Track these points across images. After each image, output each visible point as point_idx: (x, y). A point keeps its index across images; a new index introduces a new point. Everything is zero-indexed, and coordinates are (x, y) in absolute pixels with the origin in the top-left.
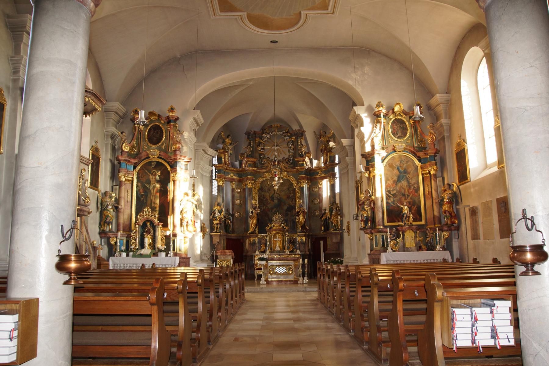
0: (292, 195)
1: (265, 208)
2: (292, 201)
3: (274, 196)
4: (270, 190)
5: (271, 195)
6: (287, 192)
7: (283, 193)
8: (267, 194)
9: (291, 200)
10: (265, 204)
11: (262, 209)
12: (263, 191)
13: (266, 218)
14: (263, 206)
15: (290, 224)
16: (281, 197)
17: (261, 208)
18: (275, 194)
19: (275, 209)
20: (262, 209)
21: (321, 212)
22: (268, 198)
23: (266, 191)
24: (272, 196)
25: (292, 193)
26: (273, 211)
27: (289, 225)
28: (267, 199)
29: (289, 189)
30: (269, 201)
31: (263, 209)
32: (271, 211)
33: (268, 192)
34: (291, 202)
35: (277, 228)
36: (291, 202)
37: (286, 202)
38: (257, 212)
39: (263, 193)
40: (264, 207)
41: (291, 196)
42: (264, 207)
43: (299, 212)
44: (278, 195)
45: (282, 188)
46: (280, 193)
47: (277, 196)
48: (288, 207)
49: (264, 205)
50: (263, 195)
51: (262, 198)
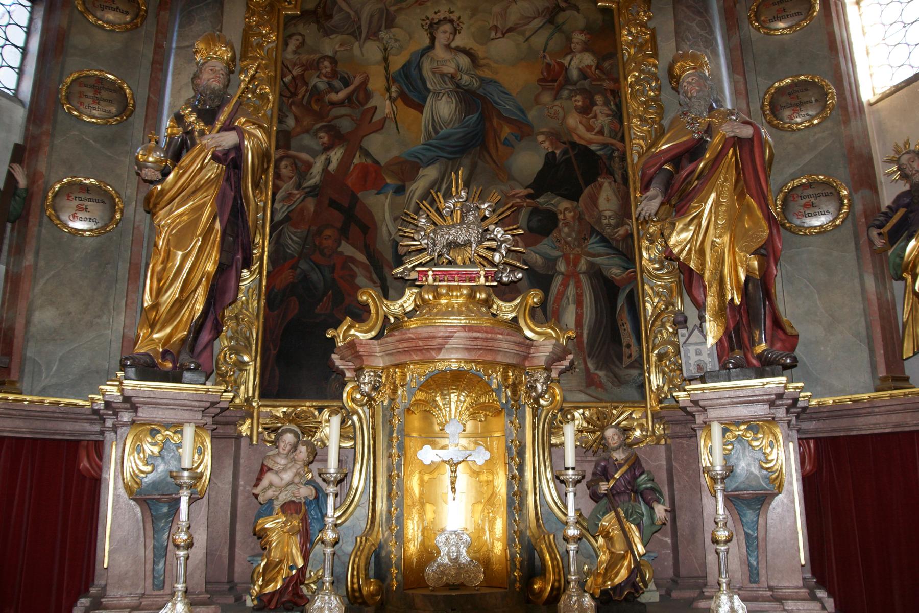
0: (588, 60)
1: (345, 162)
2: (586, 110)
3: (427, 67)
4: (390, 23)
5: (398, 62)
6: (539, 41)
7: (503, 48)
8: (372, 51)
9: (579, 100)
10: (346, 125)
11: (317, 168)
12: (327, 33)
13: (347, 249)
14: (327, 148)
15: (579, 304)
16: (486, 74)
17: (309, 166)
18: (439, 52)
19: (430, 174)
20: (317, 168)
21: (867, 192)
22: (377, 84)
23: (356, 34)
24: (406, 67)
25: (587, 48)
26: (418, 186)
27: (570, 317)
28: (363, 93)
29: (561, 18)
30: (383, 106)
31: (325, 170)
32: (400, 190)
33: (373, 34)
34: (573, 120)
35: (454, 321)
36: (573, 120)
37: (532, 115)
38: (229, 139)
39: (329, 46)
40: (336, 156)
41: (574, 73)
42: (336, 156)
43: (694, 150)
44: (464, 61)
45: (497, 9)
46: (480, 51)
47: (450, 69)
48: (550, 158)
49: (337, 137)
50: (333, 61)
51: (322, 86)
